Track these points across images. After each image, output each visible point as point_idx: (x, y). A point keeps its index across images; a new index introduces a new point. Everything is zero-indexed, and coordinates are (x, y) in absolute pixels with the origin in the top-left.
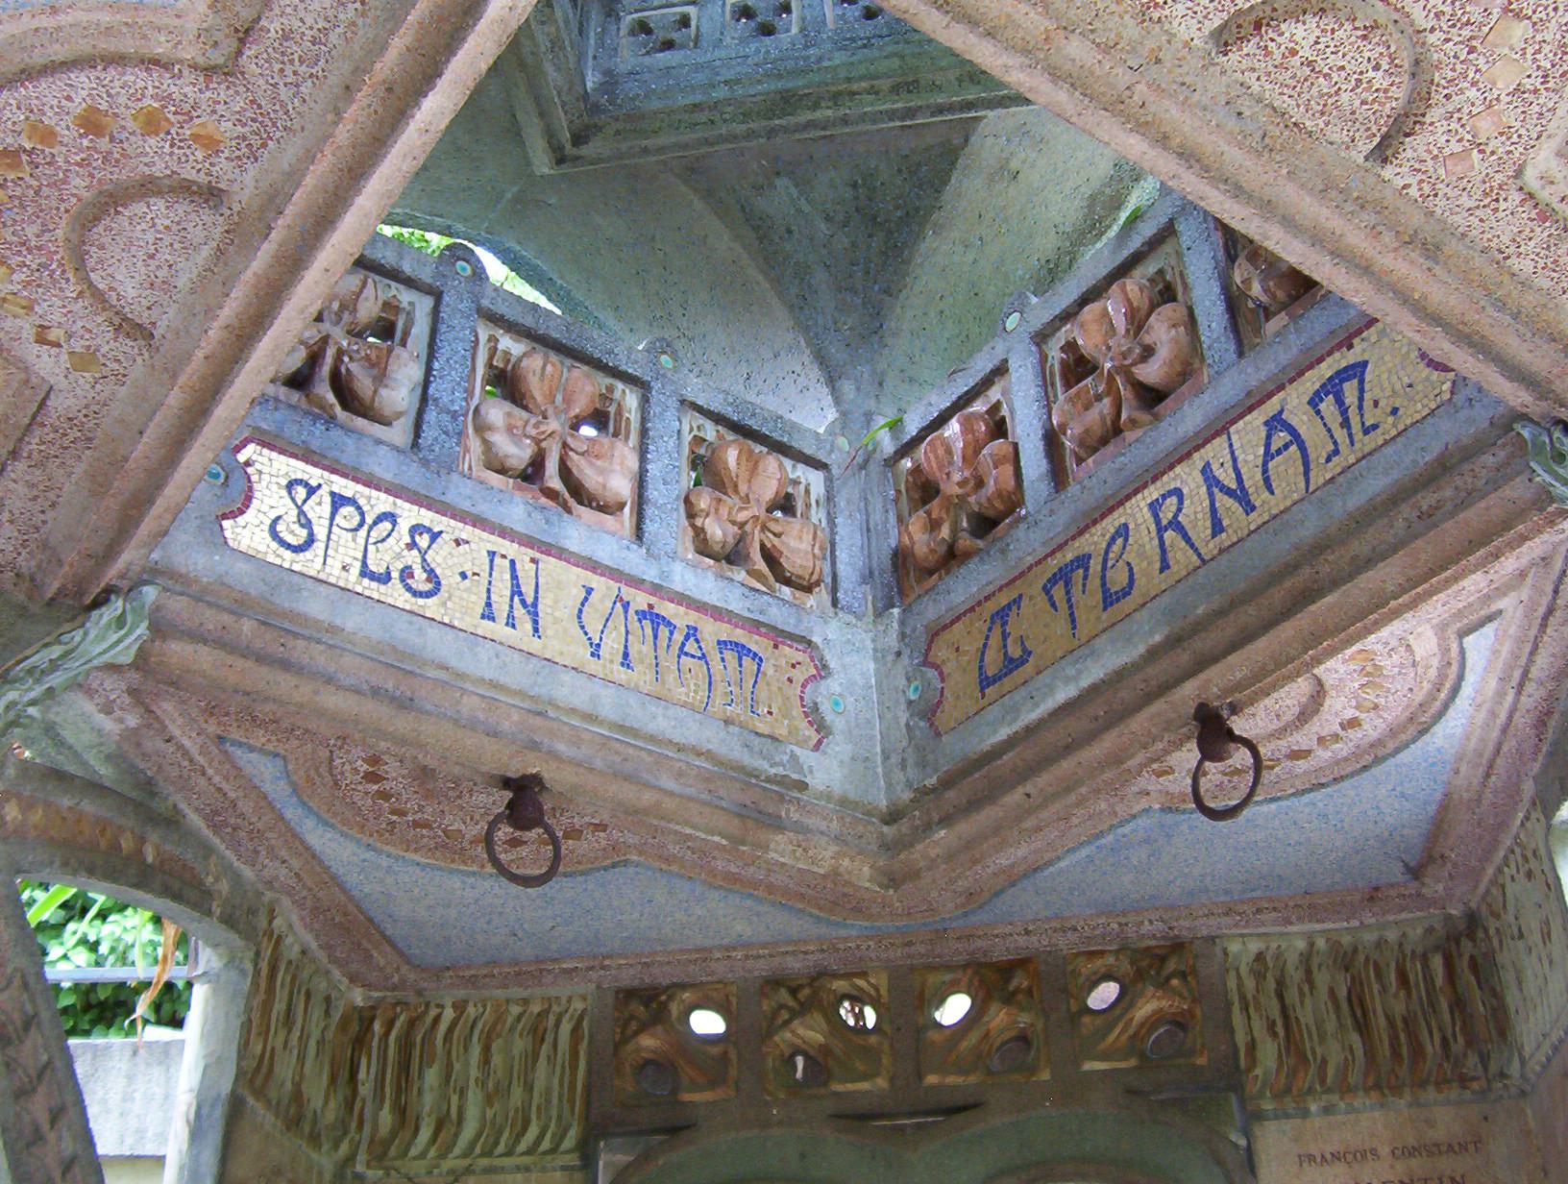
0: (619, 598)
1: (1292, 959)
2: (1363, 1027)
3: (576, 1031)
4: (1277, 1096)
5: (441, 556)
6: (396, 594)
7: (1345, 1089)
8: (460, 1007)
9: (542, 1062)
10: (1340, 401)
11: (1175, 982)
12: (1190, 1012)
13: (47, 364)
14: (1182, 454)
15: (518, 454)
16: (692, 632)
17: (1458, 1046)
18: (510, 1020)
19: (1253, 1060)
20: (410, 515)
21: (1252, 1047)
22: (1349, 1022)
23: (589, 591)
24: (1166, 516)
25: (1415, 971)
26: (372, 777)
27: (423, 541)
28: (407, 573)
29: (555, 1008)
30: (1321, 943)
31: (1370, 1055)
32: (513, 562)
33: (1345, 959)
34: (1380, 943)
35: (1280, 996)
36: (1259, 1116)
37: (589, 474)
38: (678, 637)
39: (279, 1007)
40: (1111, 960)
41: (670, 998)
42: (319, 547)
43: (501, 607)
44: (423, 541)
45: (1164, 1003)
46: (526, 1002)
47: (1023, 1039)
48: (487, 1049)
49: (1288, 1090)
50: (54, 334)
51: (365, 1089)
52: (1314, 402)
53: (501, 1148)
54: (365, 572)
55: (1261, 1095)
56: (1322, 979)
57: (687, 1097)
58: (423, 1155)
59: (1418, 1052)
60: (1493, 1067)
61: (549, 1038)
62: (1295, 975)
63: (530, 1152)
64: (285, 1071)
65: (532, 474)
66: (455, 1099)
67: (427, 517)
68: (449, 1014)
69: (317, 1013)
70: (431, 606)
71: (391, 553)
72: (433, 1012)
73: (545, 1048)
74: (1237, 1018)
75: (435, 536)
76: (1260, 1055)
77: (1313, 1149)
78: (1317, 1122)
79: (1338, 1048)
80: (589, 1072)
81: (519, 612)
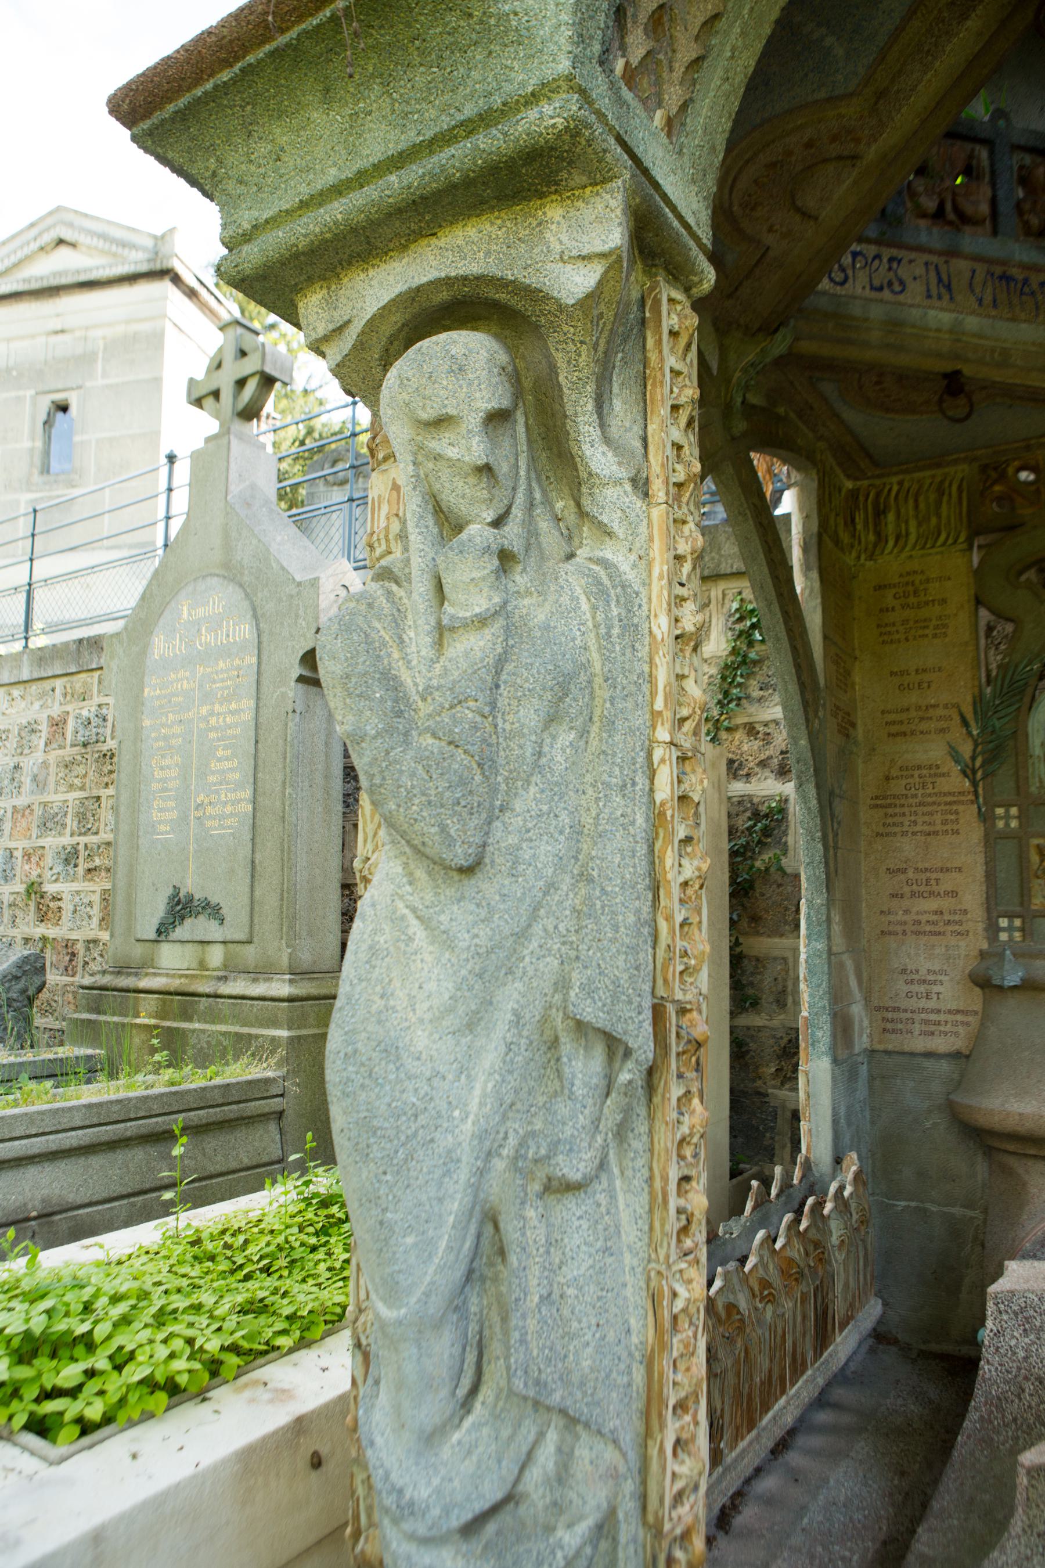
0: (988, 272)
5: (903, 272)
6: (886, 294)
8: (901, 483)
13: (769, 239)
15: (930, 204)
16: (1026, 282)
20: (887, 253)
23: (974, 272)
26: (878, 383)
27: (895, 265)
28: (890, 284)
32: (936, 266)
37: (969, 209)
38: (1019, 286)
42: (851, 280)
43: (934, 292)
44: (895, 265)
46: (933, 477)
48: (916, 501)
50: (777, 227)
51: (859, 527)
54: (872, 288)
58: (891, 553)
63: (944, 544)
65: (939, 215)
66: (903, 526)
67: (894, 252)
68: (895, 488)
70: (901, 298)
71: (882, 274)
73: (945, 498)
75: (900, 261)
80: (969, 506)
81: (943, 290)
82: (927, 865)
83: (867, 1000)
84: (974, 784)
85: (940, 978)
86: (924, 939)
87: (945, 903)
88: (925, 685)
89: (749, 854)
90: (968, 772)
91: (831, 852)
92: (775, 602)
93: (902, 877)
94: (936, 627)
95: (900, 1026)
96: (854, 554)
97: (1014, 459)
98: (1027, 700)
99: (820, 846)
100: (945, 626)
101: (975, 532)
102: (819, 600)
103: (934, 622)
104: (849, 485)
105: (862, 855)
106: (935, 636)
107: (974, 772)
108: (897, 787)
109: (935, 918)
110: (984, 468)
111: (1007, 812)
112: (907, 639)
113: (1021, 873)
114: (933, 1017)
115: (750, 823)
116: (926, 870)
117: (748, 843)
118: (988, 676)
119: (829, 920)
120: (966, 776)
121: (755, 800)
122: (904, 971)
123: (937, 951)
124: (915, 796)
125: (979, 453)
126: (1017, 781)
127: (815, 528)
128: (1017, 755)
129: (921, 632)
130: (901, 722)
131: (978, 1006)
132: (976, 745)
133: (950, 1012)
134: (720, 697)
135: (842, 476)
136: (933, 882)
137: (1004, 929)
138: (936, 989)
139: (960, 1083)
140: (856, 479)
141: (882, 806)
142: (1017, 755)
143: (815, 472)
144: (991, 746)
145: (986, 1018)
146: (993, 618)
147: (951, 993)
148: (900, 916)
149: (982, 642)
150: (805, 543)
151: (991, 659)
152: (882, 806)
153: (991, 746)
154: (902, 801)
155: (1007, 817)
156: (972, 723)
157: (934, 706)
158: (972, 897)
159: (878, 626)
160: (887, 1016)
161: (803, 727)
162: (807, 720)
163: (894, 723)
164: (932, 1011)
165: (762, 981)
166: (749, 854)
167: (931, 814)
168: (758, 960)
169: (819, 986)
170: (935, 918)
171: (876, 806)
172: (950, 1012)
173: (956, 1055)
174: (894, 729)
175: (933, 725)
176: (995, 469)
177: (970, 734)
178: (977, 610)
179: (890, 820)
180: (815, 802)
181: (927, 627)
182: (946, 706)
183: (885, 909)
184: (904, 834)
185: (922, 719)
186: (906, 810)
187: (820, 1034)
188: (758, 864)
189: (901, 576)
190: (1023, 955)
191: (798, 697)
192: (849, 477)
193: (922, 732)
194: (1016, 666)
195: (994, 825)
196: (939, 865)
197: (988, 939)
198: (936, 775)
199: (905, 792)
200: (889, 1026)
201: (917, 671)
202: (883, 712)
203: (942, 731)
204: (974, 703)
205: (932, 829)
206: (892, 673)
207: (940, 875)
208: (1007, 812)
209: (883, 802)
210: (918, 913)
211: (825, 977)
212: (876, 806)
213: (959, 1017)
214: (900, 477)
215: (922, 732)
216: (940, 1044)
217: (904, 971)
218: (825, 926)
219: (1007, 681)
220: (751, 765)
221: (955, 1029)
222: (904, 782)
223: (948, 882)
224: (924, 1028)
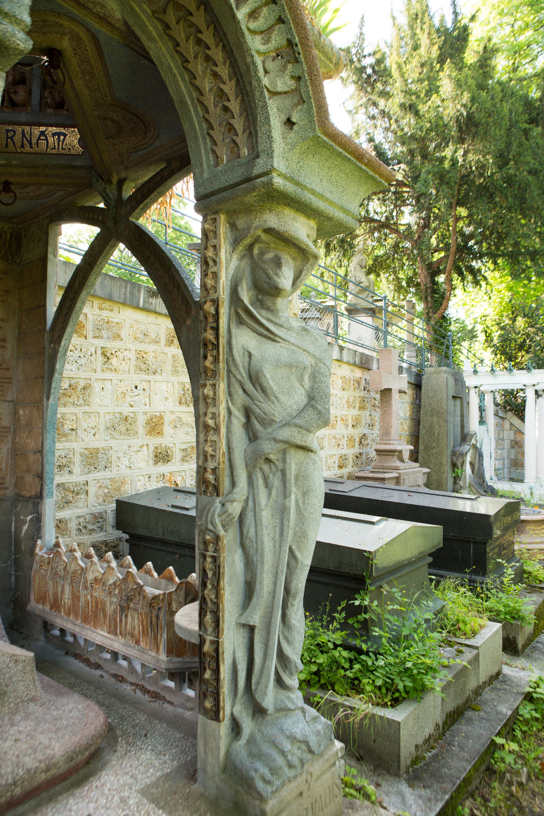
10: (59, 138)
14: (20, 124)
17: (8, 253)
24: (10, 134)
52: (54, 135)
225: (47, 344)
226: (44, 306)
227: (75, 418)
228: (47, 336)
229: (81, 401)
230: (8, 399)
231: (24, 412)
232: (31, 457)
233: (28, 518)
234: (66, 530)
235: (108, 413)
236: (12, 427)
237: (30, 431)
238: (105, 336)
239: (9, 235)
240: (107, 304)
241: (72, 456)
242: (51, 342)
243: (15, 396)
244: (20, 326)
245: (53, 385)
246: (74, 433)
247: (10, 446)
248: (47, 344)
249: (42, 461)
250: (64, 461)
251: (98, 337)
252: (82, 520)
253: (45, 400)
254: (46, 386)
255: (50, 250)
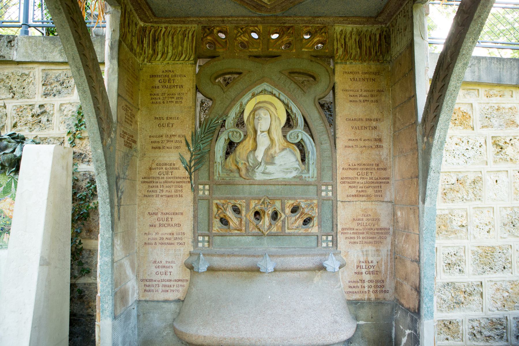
1: (348, 32)
2: (360, 48)
3: (193, 35)
4: (341, 60)
7: (354, 59)
8: (166, 28)
9: (185, 41)
11: (323, 34)
12: (326, 40)
17: (378, 54)
18: (178, 31)
19: (337, 52)
21: (337, 49)
22: (358, 46)
25: (373, 38)
29: (188, 29)
30: (355, 29)
31: (361, 53)
33: (359, 33)
34: (367, 31)
35: (345, 40)
36: (337, 63)
39: (127, 22)
40: (310, 28)
41: (214, 28)
45: (321, 38)
46: (181, 27)
47: (290, 44)
48: (173, 38)
49: (343, 58)
53: (177, 59)
55: (338, 59)
56: (353, 37)
57: (217, 50)
58: (159, 60)
59: (370, 54)
60: (385, 59)
61: (187, 36)
62: (348, 36)
63: (183, 60)
64: (129, 37)
66: (166, 48)
68: (164, 30)
69: (134, 26)
72: (160, 29)
73: (186, 39)
74: (335, 43)
76: (339, 51)
77: (347, 71)
78: (348, 65)
79: (354, 51)
80: (196, 44)
82: (167, 211)
83: (137, 276)
84: (190, 174)
85: (171, 265)
86: (164, 246)
87: (175, 230)
88: (171, 125)
89: (88, 200)
90: (188, 168)
91: (116, 208)
92: (82, 69)
93: (155, 217)
94: (178, 98)
95: (152, 288)
96: (142, 58)
97: (217, 26)
98: (215, 136)
99: (108, 206)
100: (181, 98)
101: (198, 57)
102: (117, 76)
103: (177, 96)
104: (142, 24)
105: (137, 206)
106: (177, 102)
107: (190, 168)
108: (155, 173)
109: (170, 236)
110: (204, 28)
111: (204, 187)
112: (164, 103)
113: (209, 216)
114: (168, 283)
115: (89, 185)
116: (167, 213)
117: (87, 194)
118: (200, 124)
119: (113, 245)
120: (187, 170)
121: (92, 174)
122: (155, 262)
123: (170, 252)
124: (163, 178)
125: (202, 19)
126: (209, 173)
127: (117, 37)
128: (209, 161)
129: (170, 100)
130: (159, 142)
131: (188, 278)
132: (192, 156)
133: (175, 281)
134: (77, 122)
135: (138, 18)
136: (170, 219)
137: (201, 242)
138: (169, 270)
139: (179, 313)
140: (145, 22)
141: (147, 182)
142: (209, 161)
143: (120, 8)
144: (199, 156)
145: (191, 283)
146: (204, 98)
147: (177, 271)
148: (154, 236)
149: (198, 109)
150: (111, 44)
151: (202, 116)
152: (147, 182)
153: (199, 156)
154: (157, 180)
155: (204, 189)
156: (191, 145)
157: (174, 136)
158: (187, 227)
159: (151, 95)
160: (146, 283)
161: (100, 143)
162: (102, 139)
163: (155, 142)
164: (168, 281)
165: (92, 261)
166: (88, 200)
167: (169, 187)
168: (90, 251)
169: (106, 280)
170: (170, 236)
171: (145, 182)
172: (175, 281)
173: (178, 301)
174: (155, 145)
175: (173, 144)
176: (209, 29)
177: (189, 150)
178: (196, 93)
179: (151, 189)
180: (106, 183)
181: (173, 98)
182: (179, 136)
183: (147, 232)
184: (157, 196)
185: (168, 141)
186: (159, 184)
187: (106, 306)
188: (91, 205)
189: (163, 72)
190: (208, 255)
191: (97, 126)
192: (141, 19)
193: (168, 148)
194: (212, 120)
195: (198, 193)
196: (173, 211)
197: (194, 246)
198: (173, 168)
199: (158, 176)
200: (147, 288)
201: (167, 118)
202: (150, 137)
203: (177, 148)
204: (192, 136)
205: (170, 194)
206: (155, 118)
207: (173, 216)
208: (204, 187)
209: (148, 180)
210: (162, 234)
211: (110, 276)
212: (145, 182)
213: (180, 283)
214: (166, 25)
215: (168, 148)
216: (171, 296)
217: (155, 262)
218: (110, 248)
219: (207, 127)
220: (91, 156)
221: (178, 289)
222: (158, 171)
223: (177, 219)
224: (164, 289)
225: (420, 138)
226: (415, 96)
227: (464, 214)
228: (419, 129)
229: (471, 196)
230: (386, 200)
231: (402, 214)
232: (410, 266)
233: (408, 332)
234: (457, 332)
235: (505, 208)
236: (391, 228)
237: (407, 236)
238: (496, 124)
239: (378, 36)
240: (496, 90)
241: (463, 254)
242: (424, 136)
243: (393, 197)
244: (394, 123)
245: (429, 186)
246: (464, 229)
247: (389, 248)
248: (420, 138)
249: (420, 274)
250: (454, 259)
251: (487, 127)
252: (476, 324)
253: (421, 203)
254: (421, 187)
255: (416, 32)
